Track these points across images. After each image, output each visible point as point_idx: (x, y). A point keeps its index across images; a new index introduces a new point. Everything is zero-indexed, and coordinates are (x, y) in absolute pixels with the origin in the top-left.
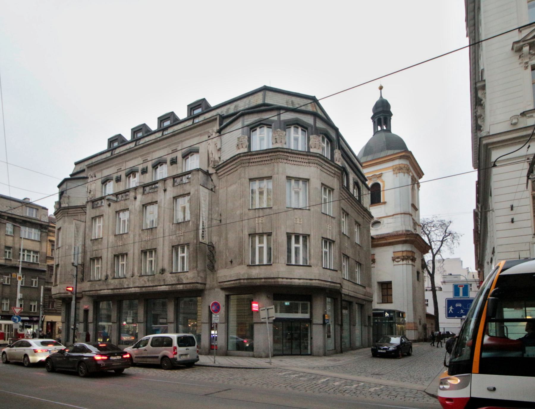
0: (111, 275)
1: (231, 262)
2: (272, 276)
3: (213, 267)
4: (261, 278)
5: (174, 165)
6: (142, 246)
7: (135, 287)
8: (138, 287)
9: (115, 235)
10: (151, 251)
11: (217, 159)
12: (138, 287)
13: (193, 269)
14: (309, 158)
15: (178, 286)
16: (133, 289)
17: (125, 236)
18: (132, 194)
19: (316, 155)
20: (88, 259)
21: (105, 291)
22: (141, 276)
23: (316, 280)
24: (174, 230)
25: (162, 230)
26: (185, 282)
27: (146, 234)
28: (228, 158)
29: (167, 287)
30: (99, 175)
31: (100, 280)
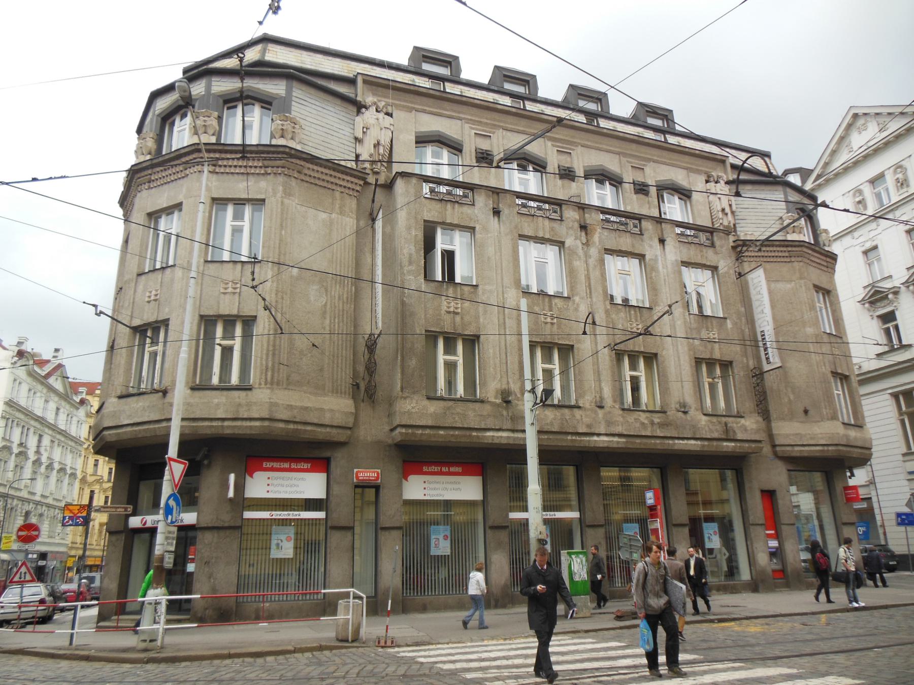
1: (806, 412)
7: (606, 435)
8: (620, 435)
12: (620, 435)
15: (725, 444)
26: (740, 436)
29: (699, 442)
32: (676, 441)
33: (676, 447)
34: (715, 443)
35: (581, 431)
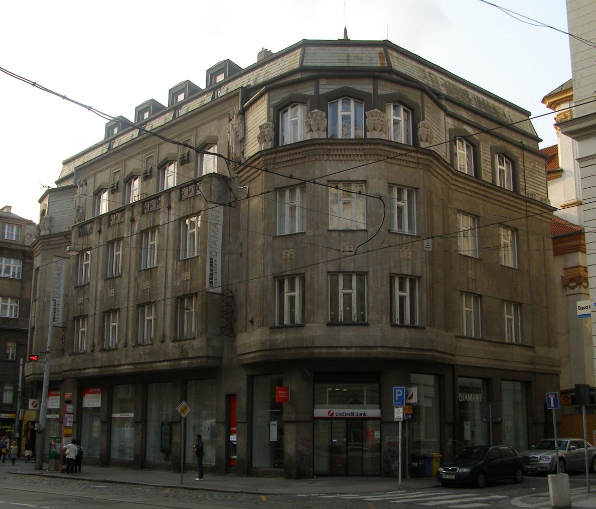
0: (99, 345)
2: (305, 345)
3: (232, 329)
4: (288, 349)
5: (186, 165)
6: (139, 298)
9: (106, 280)
10: (150, 304)
11: (239, 155)
13: (201, 334)
14: (365, 147)
15: (183, 362)
16: (126, 367)
17: (117, 280)
18: (128, 214)
19: (374, 142)
20: (71, 318)
21: (91, 370)
22: (137, 345)
23: (377, 347)
24: (178, 271)
25: (164, 272)
27: (143, 278)
28: (251, 155)
30: (91, 181)
31: (84, 353)
32: (157, 364)
33: (158, 369)
34: (177, 363)
35: (116, 364)
